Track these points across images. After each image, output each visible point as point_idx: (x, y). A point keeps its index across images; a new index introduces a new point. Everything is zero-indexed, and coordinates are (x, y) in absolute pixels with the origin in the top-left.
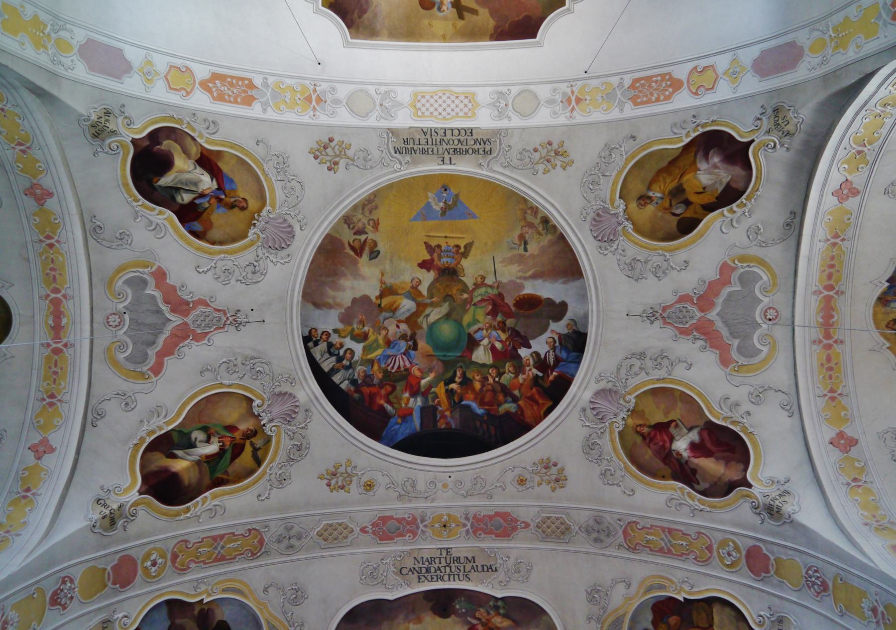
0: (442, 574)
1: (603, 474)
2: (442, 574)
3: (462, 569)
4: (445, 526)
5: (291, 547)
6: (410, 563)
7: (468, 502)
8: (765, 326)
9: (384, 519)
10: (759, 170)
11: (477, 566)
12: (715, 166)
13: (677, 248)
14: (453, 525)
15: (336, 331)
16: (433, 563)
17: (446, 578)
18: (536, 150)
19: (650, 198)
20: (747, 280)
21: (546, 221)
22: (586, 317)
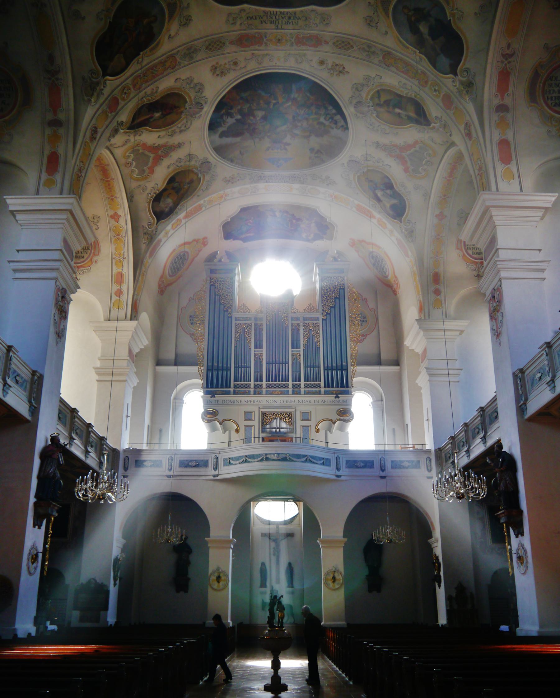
0: (281, 15)
1: (192, 81)
2: (281, 15)
3: (269, 17)
4: (279, 40)
5: (369, 47)
6: (300, 22)
7: (266, 52)
8: (130, 160)
9: (315, 46)
10: (150, 213)
11: (259, 19)
12: (166, 207)
13: (174, 171)
14: (274, 40)
15: (333, 128)
16: (286, 22)
17: (278, 13)
18: (239, 180)
19: (189, 184)
20: (142, 172)
21: (232, 161)
22: (210, 136)
